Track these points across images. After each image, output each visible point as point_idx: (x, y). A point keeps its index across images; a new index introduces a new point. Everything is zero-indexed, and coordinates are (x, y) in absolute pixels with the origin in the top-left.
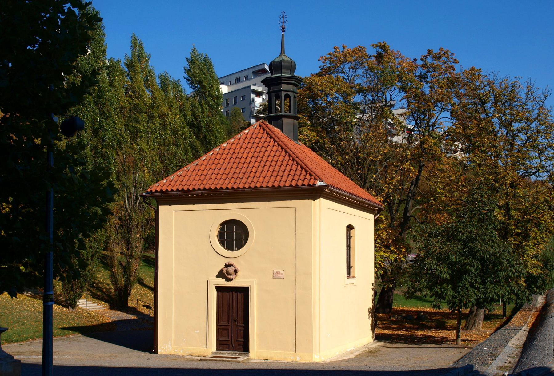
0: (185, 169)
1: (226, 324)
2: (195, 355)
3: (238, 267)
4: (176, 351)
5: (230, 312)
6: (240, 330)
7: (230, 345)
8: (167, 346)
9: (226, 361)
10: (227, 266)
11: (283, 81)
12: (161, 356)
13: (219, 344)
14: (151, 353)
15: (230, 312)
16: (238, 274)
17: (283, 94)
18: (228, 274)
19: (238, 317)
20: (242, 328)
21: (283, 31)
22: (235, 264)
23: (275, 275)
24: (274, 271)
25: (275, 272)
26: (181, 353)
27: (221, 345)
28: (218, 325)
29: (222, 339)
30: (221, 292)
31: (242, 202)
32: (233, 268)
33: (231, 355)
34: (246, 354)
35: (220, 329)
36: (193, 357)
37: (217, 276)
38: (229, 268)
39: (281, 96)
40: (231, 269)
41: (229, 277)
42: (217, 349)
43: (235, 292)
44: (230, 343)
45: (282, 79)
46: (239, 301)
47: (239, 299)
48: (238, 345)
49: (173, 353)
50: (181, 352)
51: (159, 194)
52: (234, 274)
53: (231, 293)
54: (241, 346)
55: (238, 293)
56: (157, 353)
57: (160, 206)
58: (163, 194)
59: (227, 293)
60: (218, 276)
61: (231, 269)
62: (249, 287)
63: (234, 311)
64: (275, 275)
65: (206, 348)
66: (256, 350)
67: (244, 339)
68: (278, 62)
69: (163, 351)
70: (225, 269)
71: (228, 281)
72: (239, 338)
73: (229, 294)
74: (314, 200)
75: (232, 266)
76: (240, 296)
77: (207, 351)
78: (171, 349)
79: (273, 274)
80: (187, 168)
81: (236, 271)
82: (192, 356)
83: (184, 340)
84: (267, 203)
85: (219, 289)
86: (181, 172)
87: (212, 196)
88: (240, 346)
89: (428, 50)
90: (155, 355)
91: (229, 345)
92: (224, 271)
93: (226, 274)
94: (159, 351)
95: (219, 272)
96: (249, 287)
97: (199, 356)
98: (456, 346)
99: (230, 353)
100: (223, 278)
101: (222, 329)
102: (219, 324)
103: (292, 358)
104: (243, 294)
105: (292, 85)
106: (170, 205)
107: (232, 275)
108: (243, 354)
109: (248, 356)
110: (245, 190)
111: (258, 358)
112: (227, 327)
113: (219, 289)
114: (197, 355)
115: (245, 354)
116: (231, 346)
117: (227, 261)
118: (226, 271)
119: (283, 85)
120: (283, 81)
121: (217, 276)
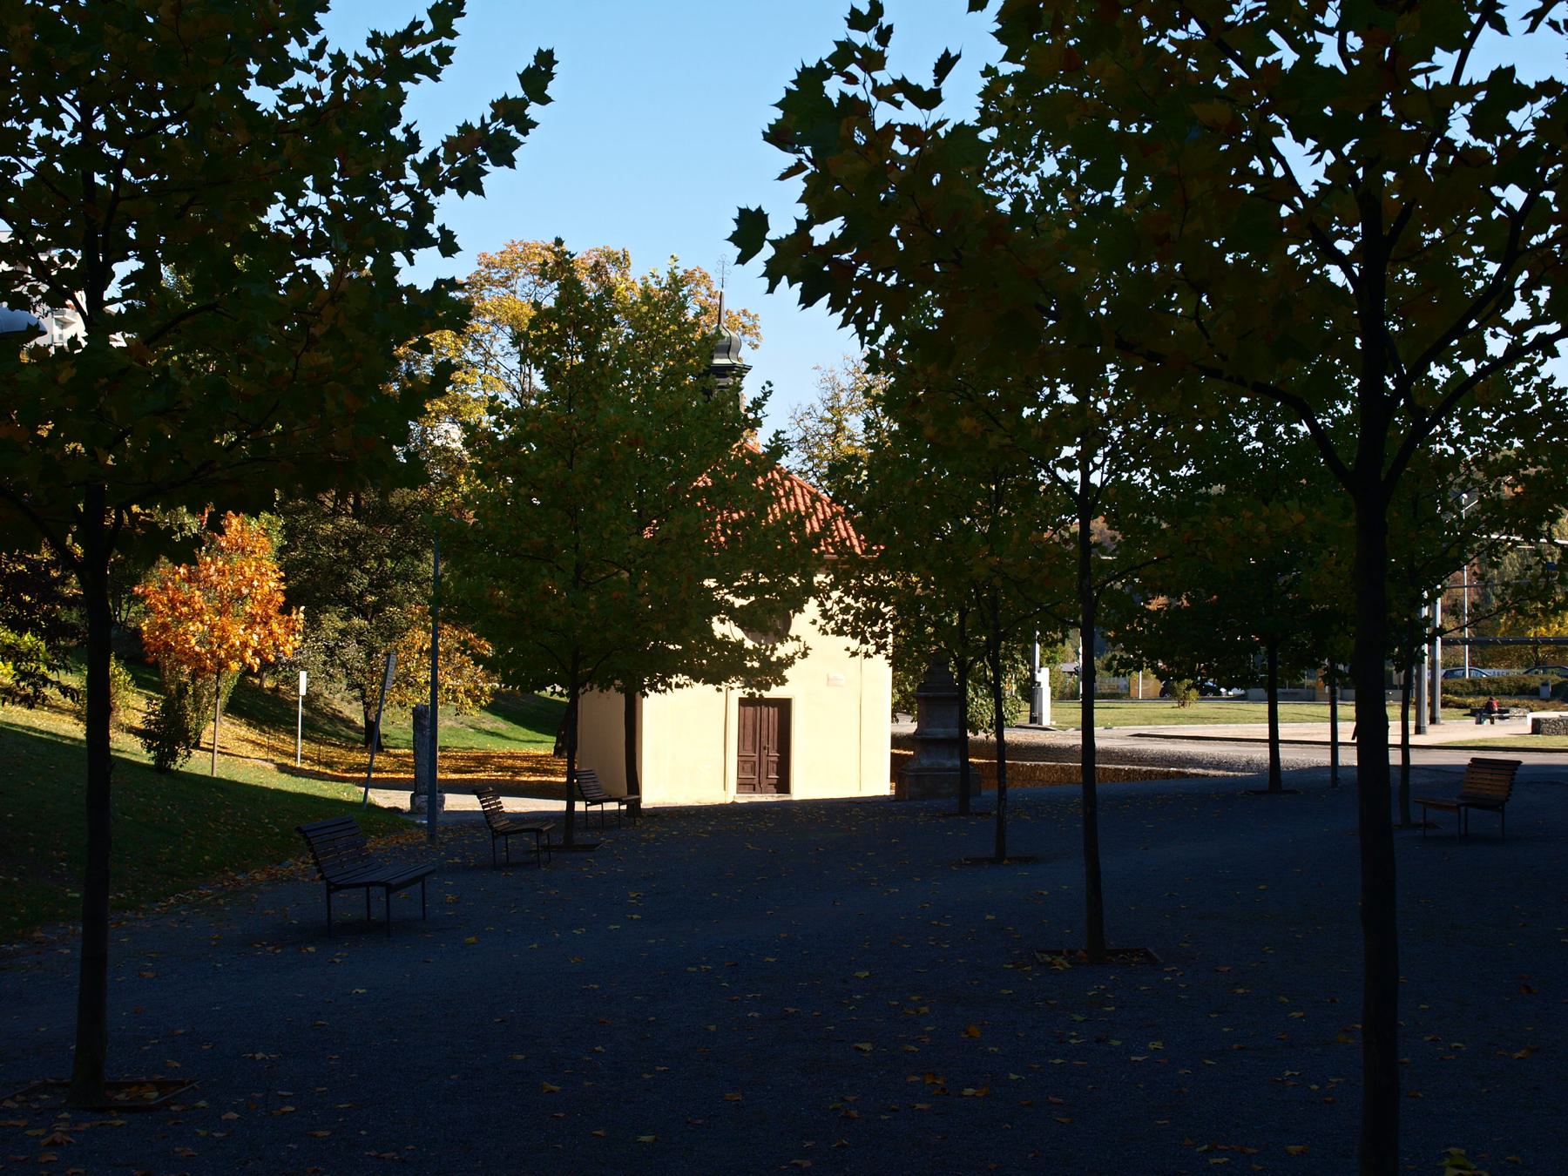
6: (773, 762)
23: (830, 681)
25: (831, 677)
27: (743, 785)
44: (756, 781)
63: (764, 733)
64: (830, 681)
76: (773, 712)
101: (745, 762)
104: (776, 709)
116: (757, 786)
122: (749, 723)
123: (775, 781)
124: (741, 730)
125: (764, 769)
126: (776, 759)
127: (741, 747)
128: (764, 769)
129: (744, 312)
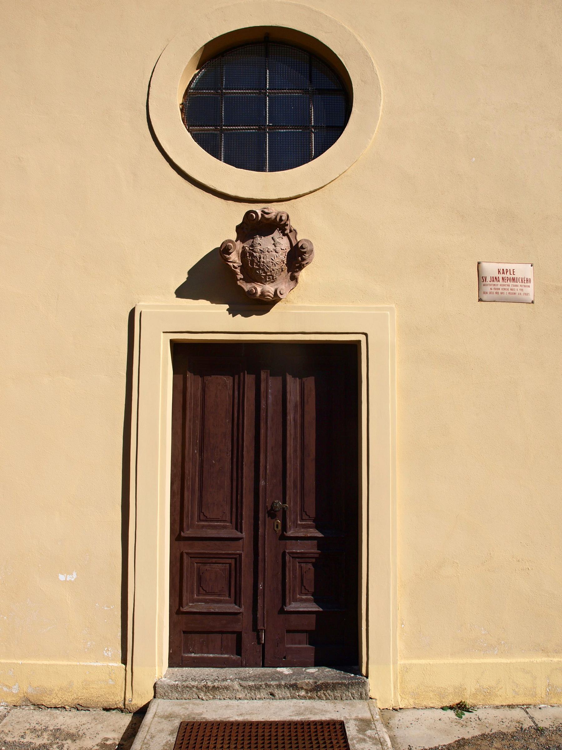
1: (223, 534)
2: (55, 701)
6: (302, 557)
7: (244, 635)
13: (184, 632)
16: (303, 275)
19: (290, 492)
20: (311, 549)
22: (293, 223)
24: (484, 265)
29: (202, 607)
32: (284, 244)
33: (263, 693)
37: (181, 292)
46: (290, 417)
47: (290, 407)
48: (288, 631)
52: (285, 275)
53: (249, 379)
54: (304, 636)
55: (289, 378)
59: (228, 380)
62: (359, 342)
66: (401, 662)
67: (317, 601)
70: (239, 245)
72: (295, 600)
73: (241, 387)
75: (277, 234)
79: (481, 279)
82: (39, 706)
88: (298, 636)
91: (239, 634)
92: (234, 258)
93: (240, 276)
95: (190, 272)
96: (359, 342)
97: (78, 707)
99: (258, 688)
100: (215, 299)
101: (204, 558)
102: (187, 533)
104: (310, 382)
107: (273, 280)
109: (364, 696)
111: (411, 702)
114: (69, 698)
115: (347, 687)
116: (248, 640)
118: (243, 255)
121: (181, 292)
123: (311, 623)
124: (192, 451)
126: (311, 549)
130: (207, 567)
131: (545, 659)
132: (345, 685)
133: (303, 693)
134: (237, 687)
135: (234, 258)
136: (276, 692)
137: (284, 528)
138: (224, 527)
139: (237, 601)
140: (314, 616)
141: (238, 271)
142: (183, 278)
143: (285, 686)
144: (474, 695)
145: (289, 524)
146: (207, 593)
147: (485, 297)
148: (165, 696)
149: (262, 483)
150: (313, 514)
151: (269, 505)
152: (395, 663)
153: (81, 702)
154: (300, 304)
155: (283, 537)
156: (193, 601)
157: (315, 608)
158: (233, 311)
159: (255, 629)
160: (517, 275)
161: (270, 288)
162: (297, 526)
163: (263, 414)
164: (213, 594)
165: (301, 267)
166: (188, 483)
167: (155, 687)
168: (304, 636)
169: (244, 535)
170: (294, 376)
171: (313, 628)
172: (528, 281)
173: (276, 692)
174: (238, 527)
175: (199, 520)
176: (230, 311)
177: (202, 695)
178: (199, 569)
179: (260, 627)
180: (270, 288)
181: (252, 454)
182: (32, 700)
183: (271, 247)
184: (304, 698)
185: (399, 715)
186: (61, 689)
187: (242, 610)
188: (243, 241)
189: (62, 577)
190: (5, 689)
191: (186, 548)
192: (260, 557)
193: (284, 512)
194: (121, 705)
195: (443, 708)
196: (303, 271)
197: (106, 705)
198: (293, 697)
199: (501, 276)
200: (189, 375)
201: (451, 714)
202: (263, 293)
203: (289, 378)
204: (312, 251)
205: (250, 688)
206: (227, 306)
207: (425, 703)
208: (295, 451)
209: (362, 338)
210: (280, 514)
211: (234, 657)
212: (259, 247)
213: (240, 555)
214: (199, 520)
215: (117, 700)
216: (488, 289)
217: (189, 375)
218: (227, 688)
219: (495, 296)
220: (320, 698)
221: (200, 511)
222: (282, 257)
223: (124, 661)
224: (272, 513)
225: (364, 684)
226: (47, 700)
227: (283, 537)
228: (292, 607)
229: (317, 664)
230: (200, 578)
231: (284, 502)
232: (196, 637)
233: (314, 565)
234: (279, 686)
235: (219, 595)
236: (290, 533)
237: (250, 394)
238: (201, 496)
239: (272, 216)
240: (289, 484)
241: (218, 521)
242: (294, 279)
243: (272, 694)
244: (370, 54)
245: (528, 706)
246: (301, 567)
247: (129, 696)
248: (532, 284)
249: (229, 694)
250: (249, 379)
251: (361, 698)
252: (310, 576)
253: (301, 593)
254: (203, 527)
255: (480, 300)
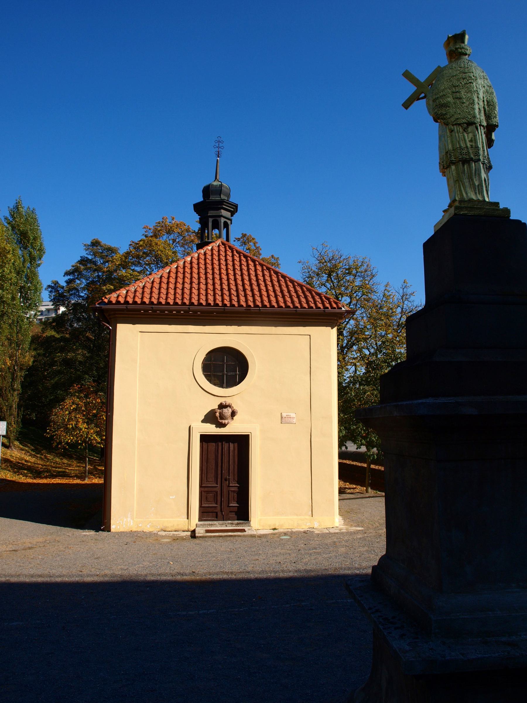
0: (148, 280)
2: (169, 530)
3: (235, 408)
4: (140, 525)
5: (219, 468)
6: (234, 491)
7: (218, 513)
8: (125, 520)
9: (235, 536)
10: (222, 406)
11: (224, 206)
12: (121, 534)
14: (97, 529)
15: (219, 468)
16: (235, 418)
17: (223, 220)
18: (222, 417)
19: (230, 474)
20: (236, 489)
21: (218, 156)
22: (233, 405)
24: (283, 414)
25: (284, 415)
26: (148, 528)
28: (201, 486)
30: (205, 442)
31: (239, 325)
33: (224, 526)
34: (247, 523)
35: (204, 491)
36: (169, 533)
37: (203, 421)
38: (225, 410)
39: (221, 222)
40: (227, 412)
41: (223, 421)
42: (200, 520)
43: (226, 442)
44: (219, 508)
45: (224, 203)
46: (231, 454)
48: (230, 512)
49: (134, 529)
50: (148, 526)
51: (124, 307)
53: (220, 444)
54: (234, 513)
55: (230, 443)
56: (109, 530)
57: (118, 325)
58: (129, 307)
59: (214, 444)
60: (204, 421)
61: (227, 412)
62: (248, 435)
63: (225, 466)
65: (186, 519)
67: (237, 503)
68: (217, 186)
69: (118, 527)
70: (219, 410)
71: (220, 427)
73: (218, 446)
74: (332, 328)
75: (228, 408)
77: (189, 524)
78: (132, 524)
79: (282, 417)
80: (150, 279)
81: (233, 414)
82: (165, 531)
83: (153, 509)
84: (273, 328)
85: (205, 439)
86: (144, 284)
87: (199, 316)
88: (232, 513)
89: (242, 234)
90: (105, 534)
91: (217, 513)
92: (218, 414)
93: (219, 418)
94: (113, 527)
95: (205, 416)
96: (248, 435)
97: (175, 531)
98: (367, 495)
99: (223, 524)
100: (212, 423)
101: (208, 492)
102: (203, 485)
103: (308, 524)
104: (236, 445)
105: (230, 213)
106: (134, 323)
107: (227, 419)
108: (242, 524)
110: (250, 309)
112: (215, 489)
113: (205, 439)
114: (174, 529)
115: (245, 523)
116: (219, 514)
117: (222, 400)
118: (220, 413)
119: (222, 211)
120: (224, 206)
121: (203, 421)
122: (212, 457)
124: (205, 463)
125: (225, 499)
126: (236, 489)
127: (204, 478)
128: (225, 499)
129: (272, 256)
130: (208, 495)
131: (297, 517)
132: (245, 523)
133: (234, 525)
134: (217, 524)
135: (218, 414)
136: (228, 525)
137: (229, 484)
138: (213, 484)
139: (216, 504)
140: (237, 507)
141: (218, 417)
142: (203, 418)
143: (230, 524)
144: (278, 526)
145: (230, 483)
146: (208, 502)
147: (282, 422)
148: (199, 527)
149: (223, 472)
150: (237, 480)
151: (225, 477)
152: (258, 518)
153: (176, 530)
154: (235, 425)
155: (229, 486)
156: (205, 504)
157: (237, 505)
158: (216, 427)
159: (221, 511)
160: (291, 416)
161: (226, 421)
162: (232, 483)
163: (223, 453)
164: (210, 502)
165: (234, 416)
166: (203, 472)
167: (196, 525)
168: (234, 513)
169: (218, 486)
170: (232, 443)
171: (236, 511)
172: (294, 418)
173: (228, 525)
174: (217, 484)
175: (206, 482)
176: (216, 427)
177: (208, 526)
178: (206, 495)
179: (223, 510)
180: (226, 421)
181: (221, 464)
182: (164, 529)
183: (227, 411)
184: (234, 526)
185: (258, 531)
186: (171, 526)
187: (218, 506)
188: (220, 410)
189: (171, 497)
190: (156, 527)
191: (203, 489)
192: (223, 492)
193: (229, 479)
194: (187, 530)
195: (270, 529)
196: (235, 417)
197: (183, 530)
198: (232, 526)
199: (287, 417)
200: (204, 443)
201: (272, 530)
202: (225, 423)
203: (230, 443)
204: (237, 412)
205: (221, 524)
206: (215, 425)
207: (265, 528)
208: (232, 463)
209: (250, 434)
210: (228, 480)
211: (215, 519)
212: (224, 412)
213: (217, 491)
214: (206, 482)
215: (186, 529)
216: (283, 420)
217: (204, 443)
218: (215, 524)
219: (285, 422)
220: (239, 526)
221: (207, 478)
222: (230, 414)
223: (188, 518)
224: (226, 480)
225: (250, 523)
226: (167, 530)
227: (229, 486)
228: (231, 505)
229: (237, 520)
230: (206, 498)
231: (229, 477)
232: (205, 513)
233: (237, 493)
234: (228, 524)
235: (212, 502)
236: (231, 485)
237: (220, 448)
238: (207, 475)
239: (228, 404)
240: (230, 472)
241: (211, 482)
242: (232, 419)
243: (226, 526)
244: (254, 355)
245: (292, 529)
246: (233, 495)
247: (189, 527)
248: (295, 419)
249: (215, 526)
250: (220, 444)
251: (249, 526)
252: (236, 496)
253: (233, 501)
254: (208, 484)
255: (281, 423)
